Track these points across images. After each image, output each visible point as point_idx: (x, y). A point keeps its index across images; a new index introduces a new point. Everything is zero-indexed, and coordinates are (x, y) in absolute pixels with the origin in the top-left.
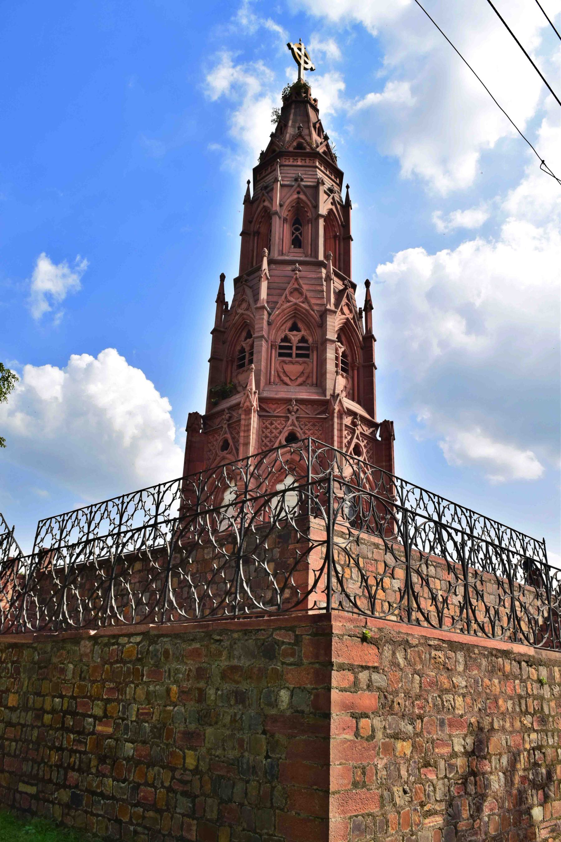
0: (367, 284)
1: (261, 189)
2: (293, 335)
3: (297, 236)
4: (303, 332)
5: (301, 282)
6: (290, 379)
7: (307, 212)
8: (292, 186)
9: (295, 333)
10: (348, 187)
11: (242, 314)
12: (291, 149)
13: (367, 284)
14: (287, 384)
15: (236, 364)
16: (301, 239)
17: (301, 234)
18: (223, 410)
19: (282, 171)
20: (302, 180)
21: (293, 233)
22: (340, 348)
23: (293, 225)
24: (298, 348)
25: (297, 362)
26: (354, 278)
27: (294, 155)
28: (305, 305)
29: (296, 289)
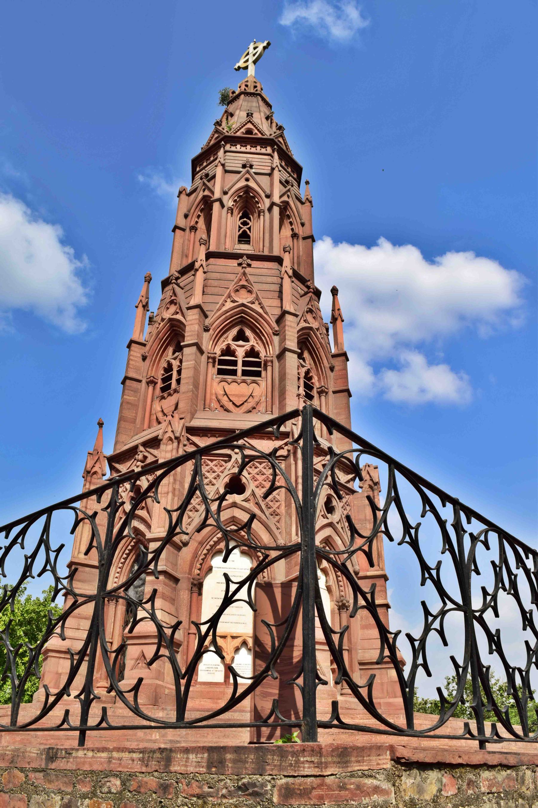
0: (334, 291)
1: (201, 179)
2: (238, 346)
3: (245, 231)
4: (251, 343)
5: (251, 279)
6: (233, 403)
7: (258, 202)
8: (239, 172)
9: (241, 343)
10: (307, 183)
11: (170, 320)
12: (238, 134)
13: (334, 291)
14: (227, 410)
15: (160, 385)
16: (251, 235)
17: (249, 229)
18: (136, 447)
19: (227, 157)
20: (251, 167)
21: (240, 228)
22: (303, 366)
23: (240, 220)
24: (245, 364)
25: (244, 381)
26: (318, 283)
27: (242, 141)
28: (256, 307)
29: (243, 287)
